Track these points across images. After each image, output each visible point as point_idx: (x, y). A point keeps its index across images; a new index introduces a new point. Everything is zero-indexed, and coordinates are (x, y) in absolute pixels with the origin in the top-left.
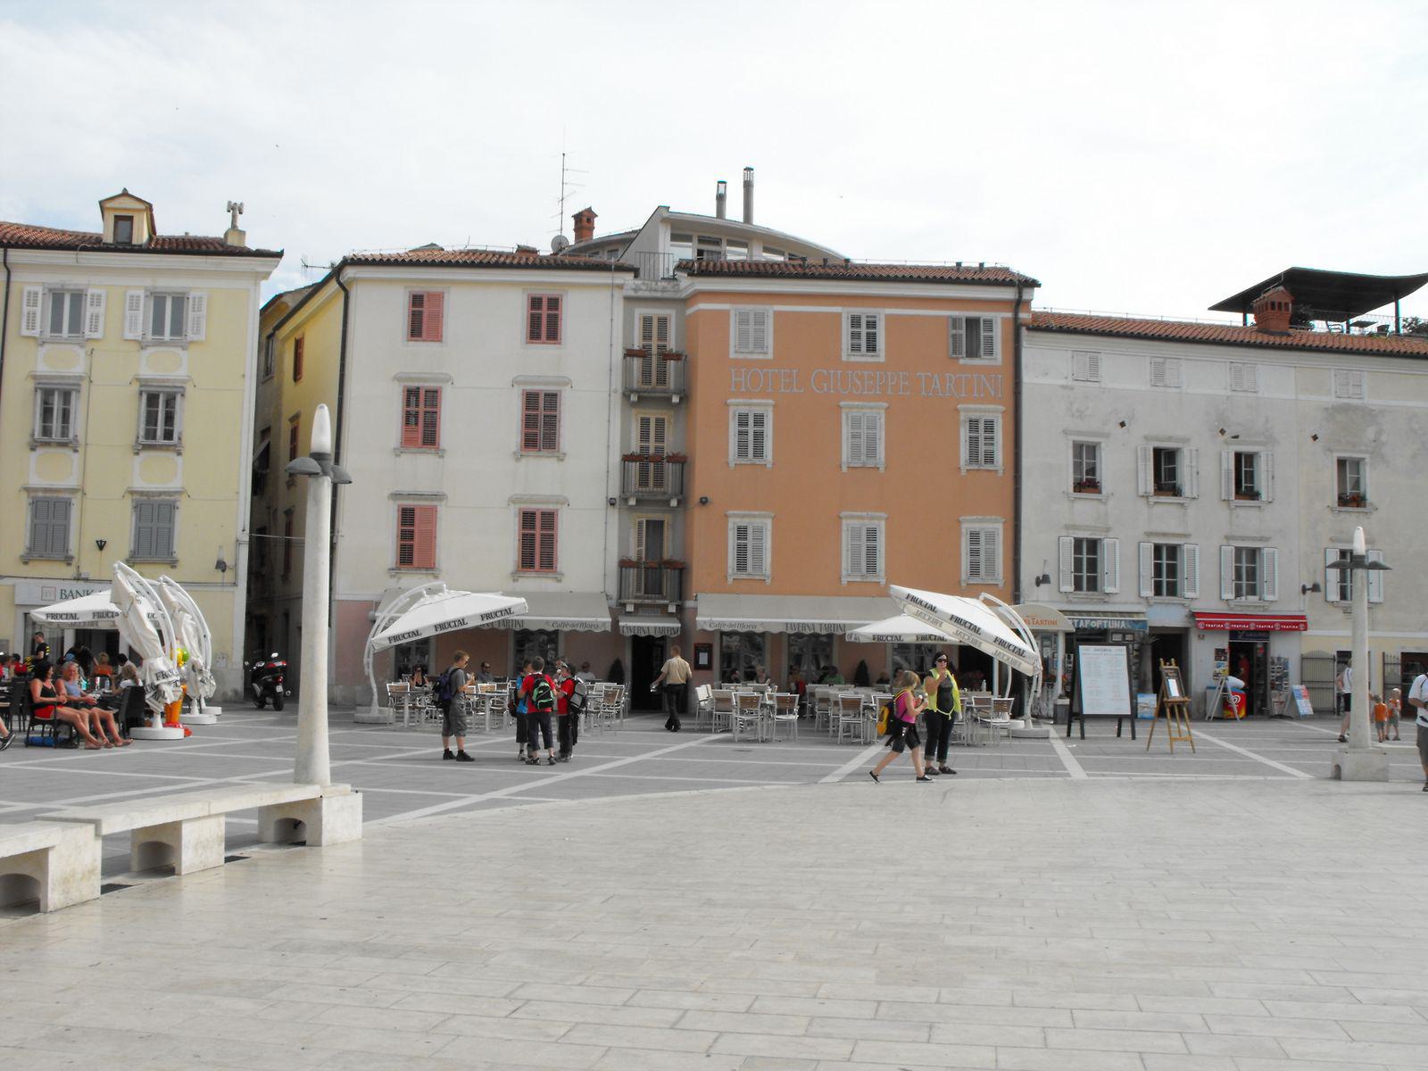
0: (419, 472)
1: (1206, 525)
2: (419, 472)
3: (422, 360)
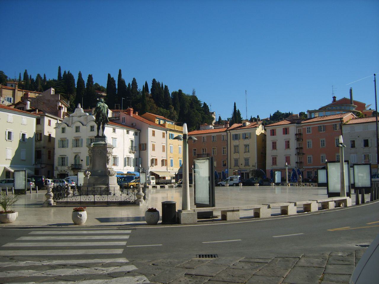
0: (274, 152)
2: (274, 152)
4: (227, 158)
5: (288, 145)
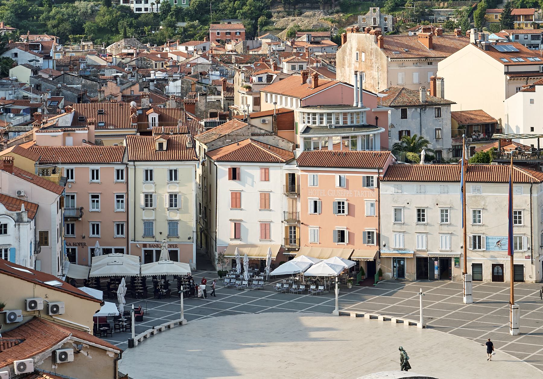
2: (237, 215)
3: (235, 185)
5: (265, 201)
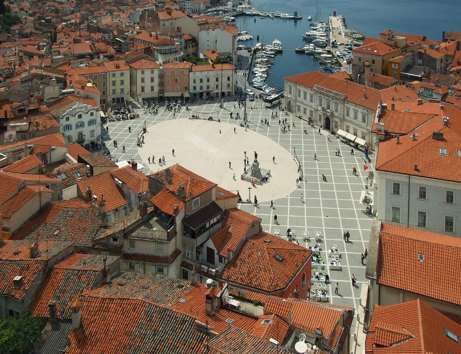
0: (143, 84)
1: (205, 84)
2: (143, 84)
3: (143, 76)
4: (106, 89)
5: (152, 80)
